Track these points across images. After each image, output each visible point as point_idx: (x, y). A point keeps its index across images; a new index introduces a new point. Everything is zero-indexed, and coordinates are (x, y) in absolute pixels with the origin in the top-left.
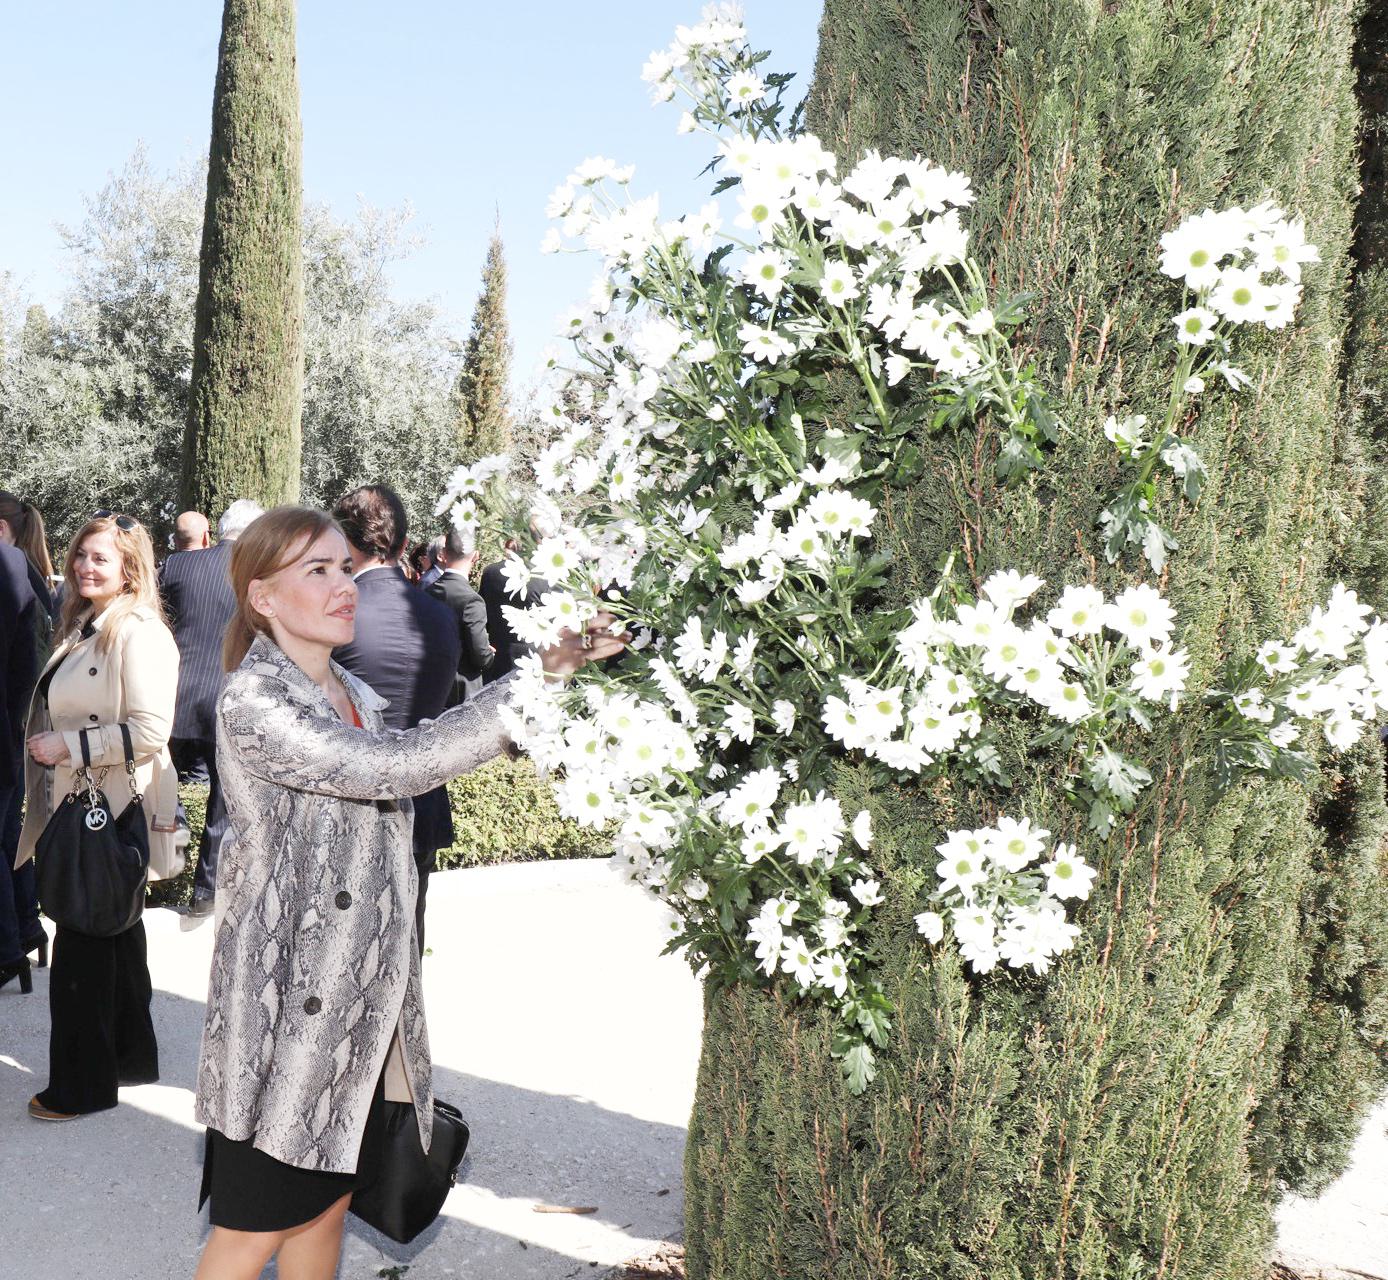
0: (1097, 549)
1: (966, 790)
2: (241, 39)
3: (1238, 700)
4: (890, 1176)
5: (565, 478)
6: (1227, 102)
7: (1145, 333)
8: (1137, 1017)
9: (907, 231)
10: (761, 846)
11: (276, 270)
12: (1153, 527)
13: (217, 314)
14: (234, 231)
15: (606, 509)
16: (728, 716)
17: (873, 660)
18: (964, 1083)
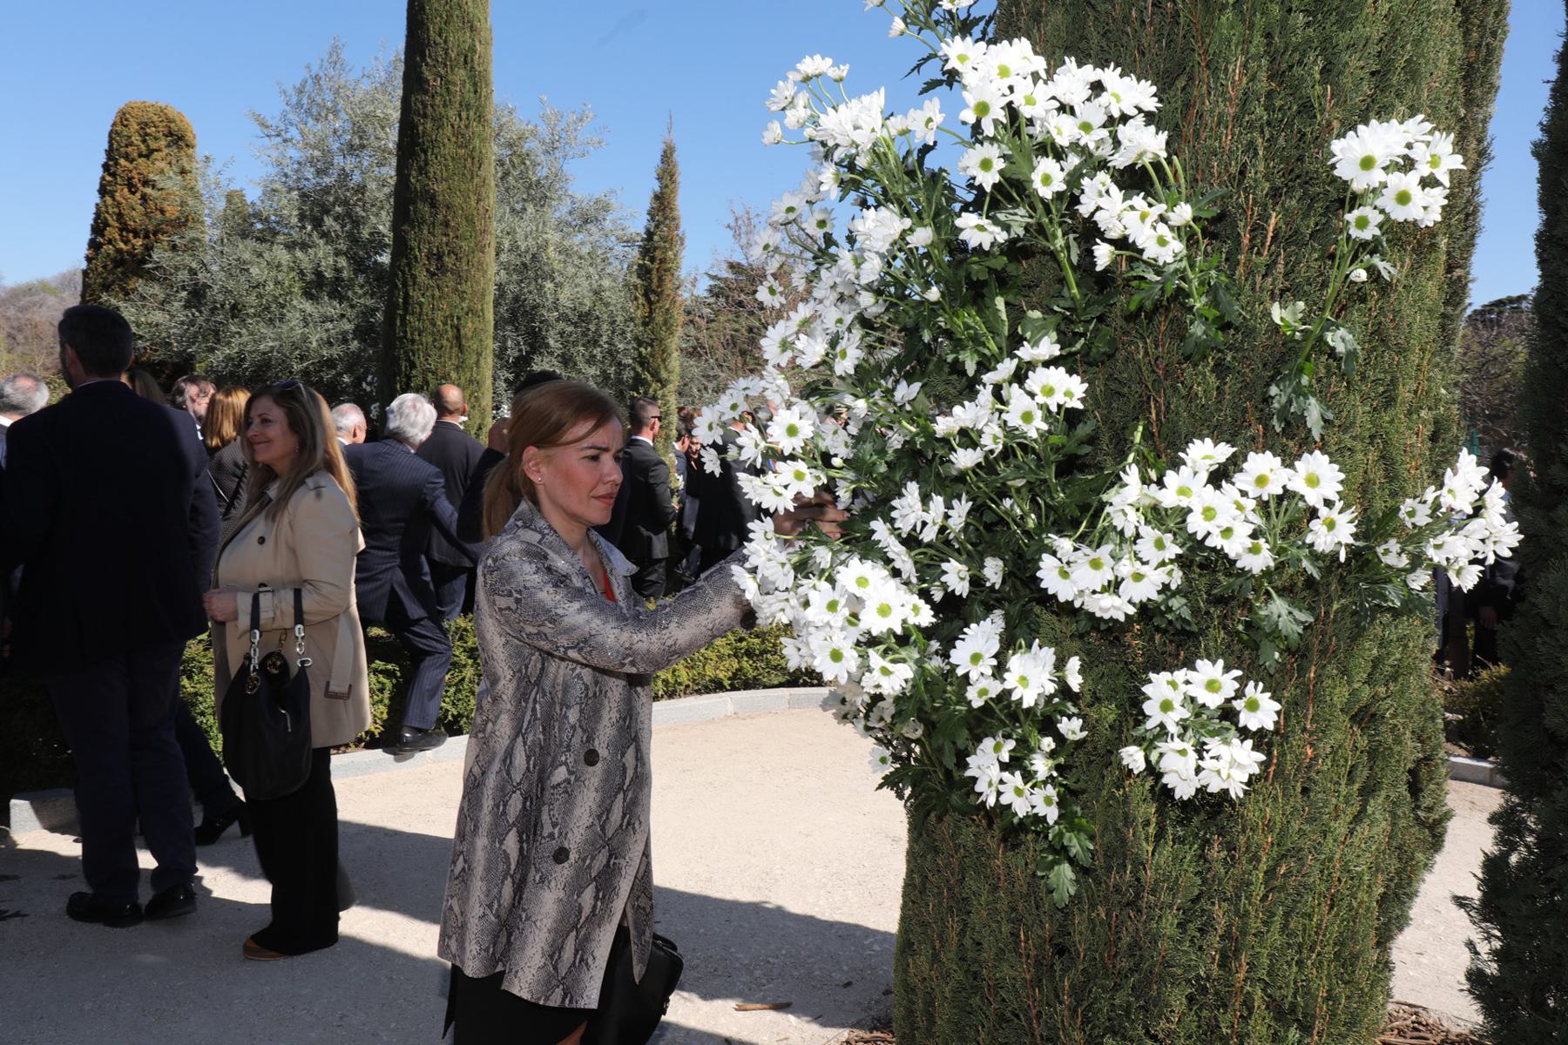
0: (1265, 420)
1: (1163, 636)
3: (1380, 550)
4: (1089, 977)
5: (789, 354)
7: (1303, 229)
8: (1295, 825)
9: (1105, 133)
10: (983, 692)
12: (1312, 400)
13: (414, 203)
14: (429, 125)
15: (828, 383)
16: (944, 572)
17: (1084, 519)
18: (1153, 892)
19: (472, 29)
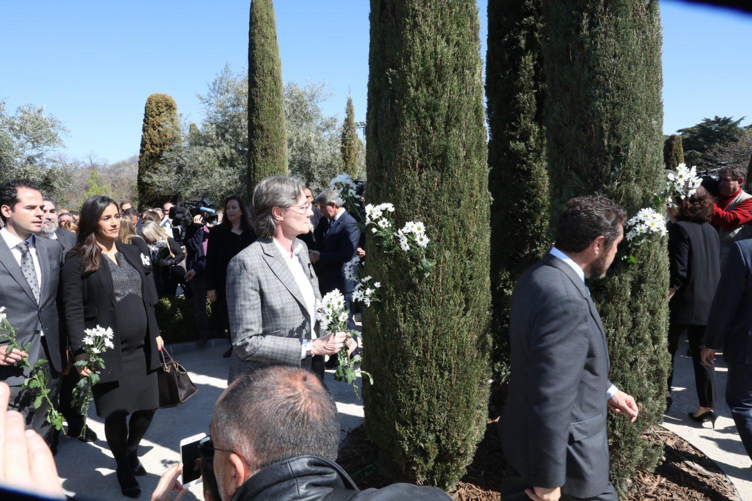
2: (256, 31)
6: (443, 111)
11: (275, 113)
13: (255, 130)
14: (259, 100)
19: (272, 61)
